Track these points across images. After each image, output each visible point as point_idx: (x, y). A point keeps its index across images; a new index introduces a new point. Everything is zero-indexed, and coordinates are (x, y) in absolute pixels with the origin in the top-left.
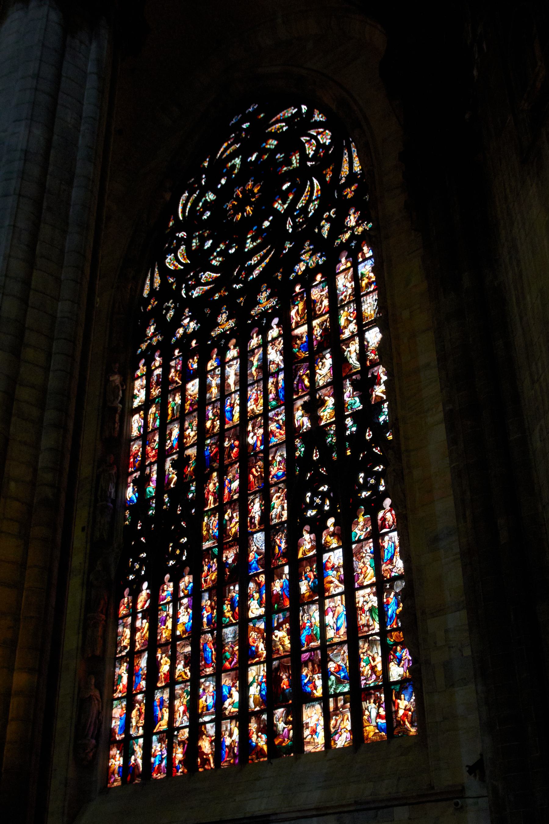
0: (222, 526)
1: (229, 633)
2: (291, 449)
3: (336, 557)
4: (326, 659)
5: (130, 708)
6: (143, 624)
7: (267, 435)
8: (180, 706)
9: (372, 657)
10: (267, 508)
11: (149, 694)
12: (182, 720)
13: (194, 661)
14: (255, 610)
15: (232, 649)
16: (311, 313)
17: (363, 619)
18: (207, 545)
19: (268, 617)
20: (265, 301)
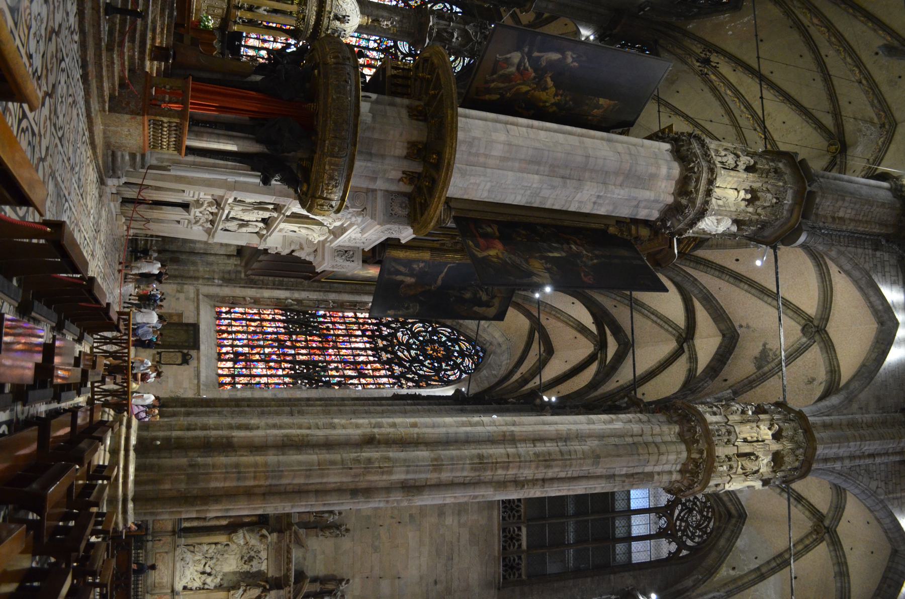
0: (300, 341)
1: (261, 343)
2: (322, 362)
3: (280, 372)
4: (246, 368)
5: (242, 313)
6: (270, 317)
7: (331, 355)
8: (240, 328)
9: (244, 380)
10: (303, 355)
11: (246, 320)
12: (234, 329)
13: (255, 332)
14: (267, 350)
15: (256, 343)
16: (374, 370)
17: (257, 379)
18: (294, 337)
19: (264, 354)
20: (385, 356)
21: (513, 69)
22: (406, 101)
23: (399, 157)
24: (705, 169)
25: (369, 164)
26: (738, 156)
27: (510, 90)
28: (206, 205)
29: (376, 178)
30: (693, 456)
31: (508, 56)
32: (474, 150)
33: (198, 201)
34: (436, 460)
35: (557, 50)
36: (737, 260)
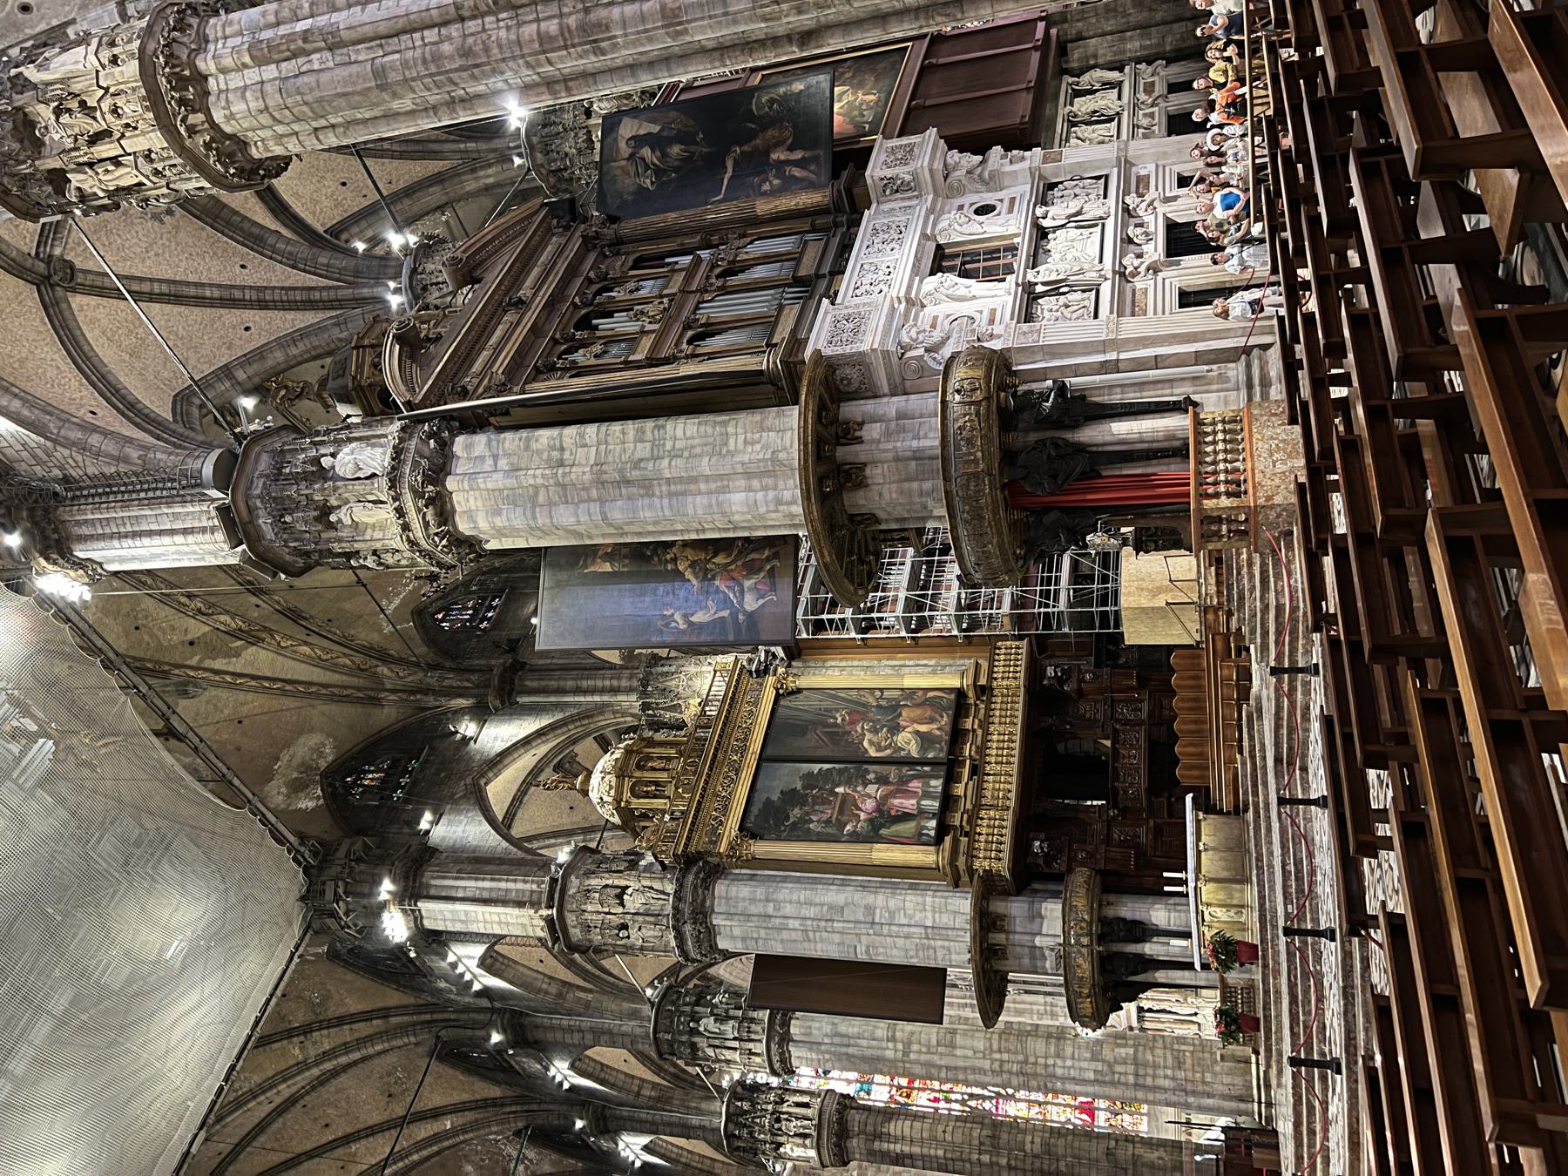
21: (747, 583)
22: (883, 527)
23: (875, 463)
24: (423, 542)
25: (915, 444)
26: (380, 564)
27: (740, 552)
28: (1142, 269)
29: (898, 418)
30: (200, 117)
31: (761, 602)
32: (771, 494)
33: (1155, 272)
34: (679, 34)
35: (701, 626)
36: (247, 329)
